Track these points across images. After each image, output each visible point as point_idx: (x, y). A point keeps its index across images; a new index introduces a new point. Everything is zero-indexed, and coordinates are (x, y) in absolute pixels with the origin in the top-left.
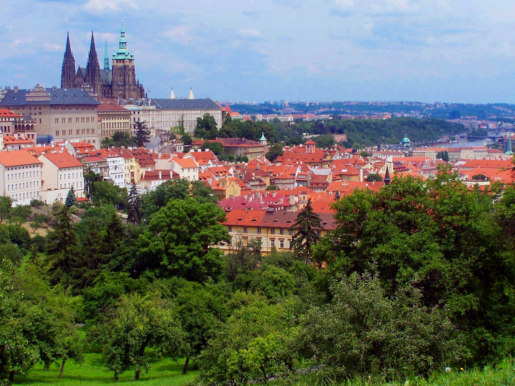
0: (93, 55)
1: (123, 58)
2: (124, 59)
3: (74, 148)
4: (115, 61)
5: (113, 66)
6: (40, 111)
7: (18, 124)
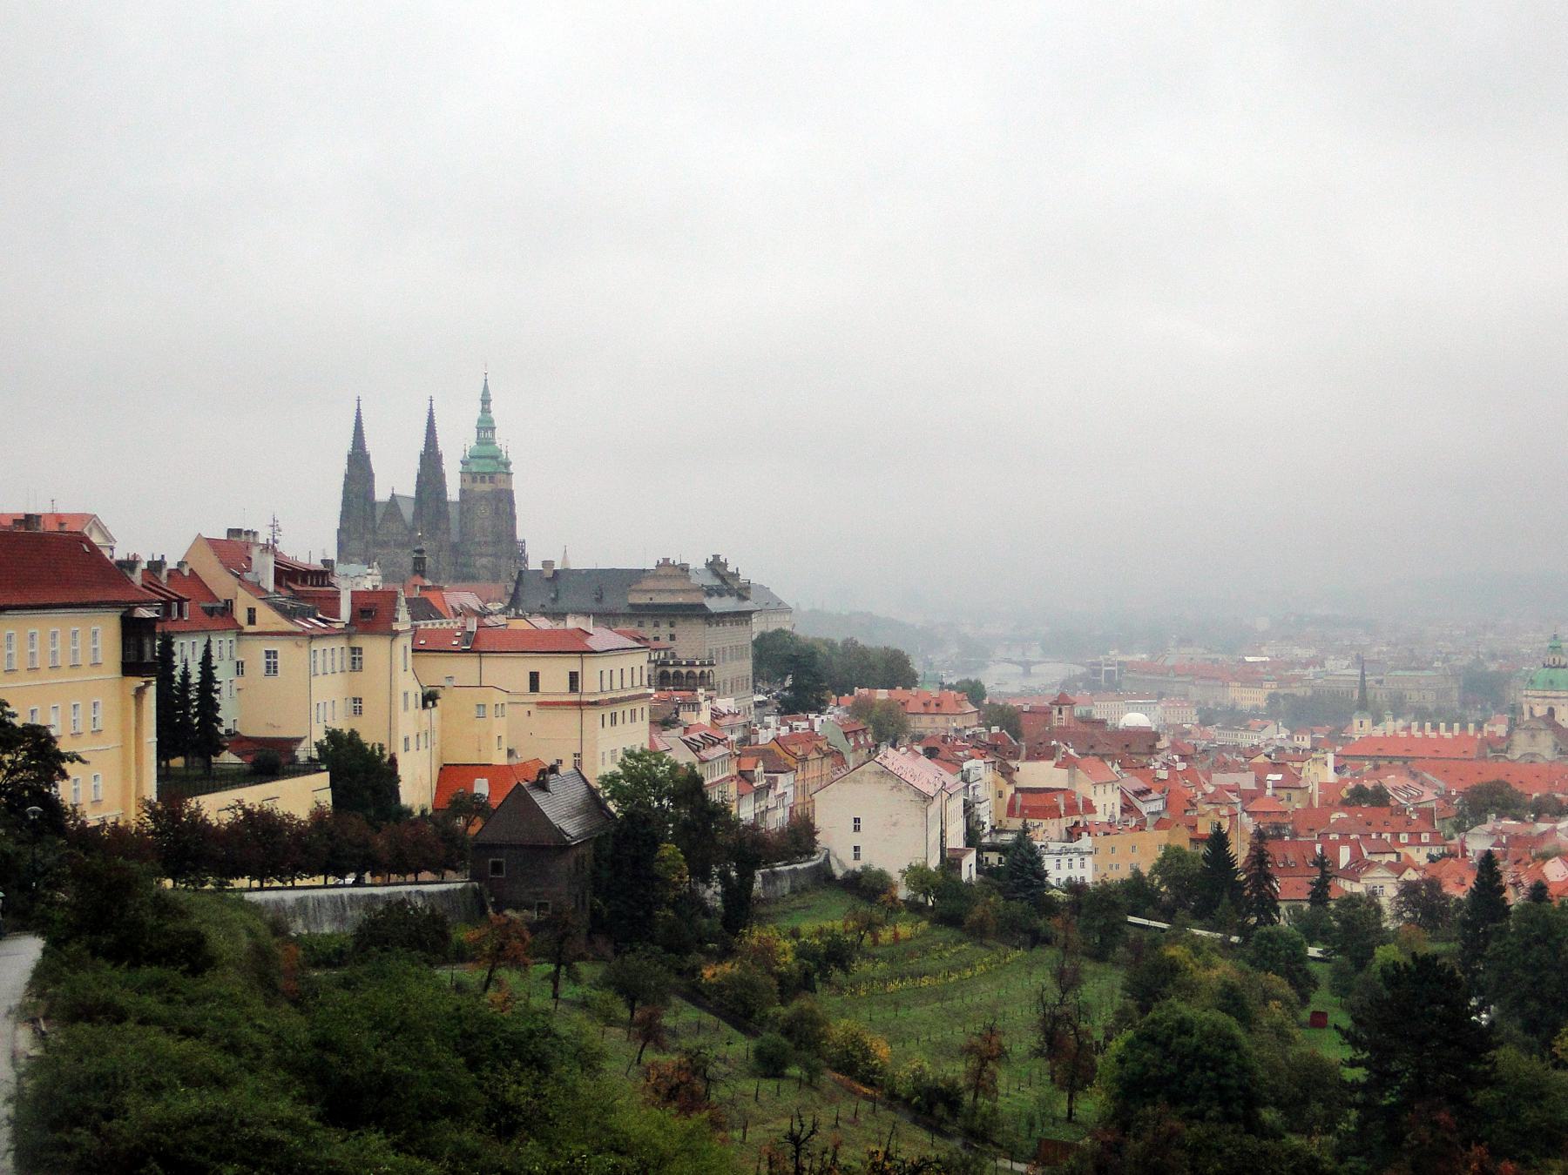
0: (431, 459)
1: (488, 470)
2: (495, 473)
3: (846, 734)
4: (469, 478)
5: (462, 492)
6: (673, 631)
7: (671, 670)
